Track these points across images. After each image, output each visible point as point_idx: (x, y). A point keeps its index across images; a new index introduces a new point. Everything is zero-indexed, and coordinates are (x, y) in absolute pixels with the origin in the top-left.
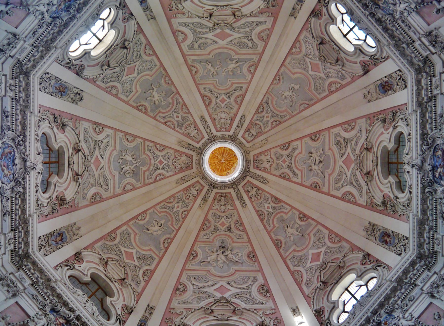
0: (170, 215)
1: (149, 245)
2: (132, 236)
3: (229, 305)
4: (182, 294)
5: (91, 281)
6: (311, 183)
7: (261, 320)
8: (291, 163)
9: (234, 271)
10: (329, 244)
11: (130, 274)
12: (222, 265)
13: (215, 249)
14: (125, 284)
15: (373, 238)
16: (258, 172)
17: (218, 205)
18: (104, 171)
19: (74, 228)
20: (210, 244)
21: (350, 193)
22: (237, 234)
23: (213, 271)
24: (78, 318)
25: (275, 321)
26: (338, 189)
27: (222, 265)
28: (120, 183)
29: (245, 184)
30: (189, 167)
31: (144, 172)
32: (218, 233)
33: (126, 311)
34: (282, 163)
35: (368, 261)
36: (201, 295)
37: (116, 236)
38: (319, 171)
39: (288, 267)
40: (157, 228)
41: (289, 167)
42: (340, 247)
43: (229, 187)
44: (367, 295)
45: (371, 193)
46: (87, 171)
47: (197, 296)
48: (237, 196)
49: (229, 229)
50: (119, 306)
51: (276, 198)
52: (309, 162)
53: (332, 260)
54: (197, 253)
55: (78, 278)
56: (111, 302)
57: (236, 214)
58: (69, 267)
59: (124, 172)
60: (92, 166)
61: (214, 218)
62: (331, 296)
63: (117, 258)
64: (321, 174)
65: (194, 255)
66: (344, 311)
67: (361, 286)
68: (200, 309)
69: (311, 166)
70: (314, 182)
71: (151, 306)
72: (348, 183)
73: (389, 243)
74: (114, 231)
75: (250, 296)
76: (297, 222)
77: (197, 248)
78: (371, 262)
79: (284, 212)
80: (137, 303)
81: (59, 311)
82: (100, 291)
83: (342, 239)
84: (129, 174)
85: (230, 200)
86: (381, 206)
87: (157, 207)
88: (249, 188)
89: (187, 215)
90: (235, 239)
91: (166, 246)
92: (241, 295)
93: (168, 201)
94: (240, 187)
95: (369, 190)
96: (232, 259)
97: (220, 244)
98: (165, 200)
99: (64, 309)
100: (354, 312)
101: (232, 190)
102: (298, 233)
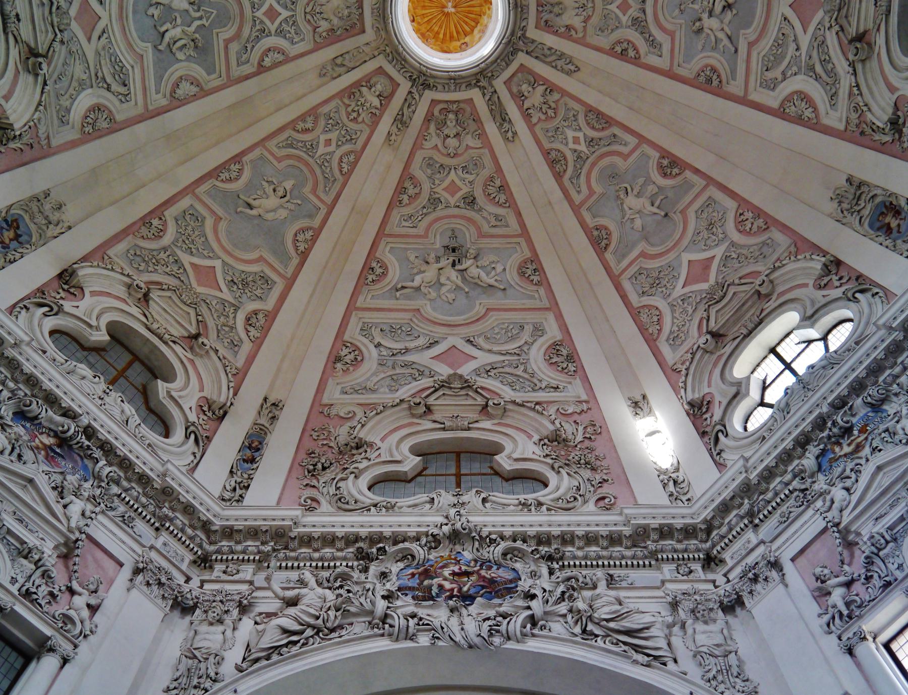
0: (307, 164)
1: (257, 247)
2: (209, 223)
3: (470, 393)
4: (351, 369)
5: (109, 343)
6: (697, 68)
7: (551, 427)
8: (644, 12)
9: (484, 311)
10: (736, 236)
11: (211, 324)
12: (451, 296)
13: (433, 255)
14: (200, 347)
15: (854, 220)
16: (550, 40)
17: (438, 135)
18: (111, 42)
19: (47, 207)
20: (419, 241)
21: (804, 97)
22: (490, 214)
23: (428, 310)
24: (89, 432)
25: (589, 430)
26: (772, 85)
27: (451, 296)
28: (161, 77)
29: (513, 75)
30: (354, 28)
31: (227, 42)
32: (439, 213)
33: (210, 414)
34: (617, 11)
35: (835, 278)
36: (398, 370)
37: (165, 224)
38: (721, 35)
39: (624, 297)
40: (272, 201)
41: (638, 23)
42: (764, 243)
43: (469, 86)
44: (824, 363)
45: (861, 94)
46: (62, 42)
48: (491, 111)
49: (470, 201)
50: (190, 401)
51: (599, 114)
52: (696, 7)
53: (740, 278)
54: (384, 267)
55: (74, 334)
56: (168, 392)
57: (487, 160)
58: (46, 309)
59: (169, 45)
60: (74, 26)
61: (429, 171)
62: (732, 368)
63: (173, 282)
64: (726, 41)
65: (379, 271)
66: (762, 404)
67: (809, 342)
68: (398, 405)
69: (700, 20)
70: (706, 66)
71: (272, 399)
72: (800, 69)
73: (895, 231)
74: (158, 211)
75: (525, 371)
76: (654, 179)
77: (385, 253)
78: (844, 281)
79: (619, 154)
80: (235, 394)
81: (36, 418)
82: (137, 366)
83: (770, 222)
84: (185, 50)
85: (471, 122)
86: (887, 130)
87: (272, 144)
88: (525, 87)
89: (354, 165)
90: (486, 228)
91: (302, 248)
92: (501, 370)
93: (299, 127)
94: (499, 84)
95: (858, 86)
96: (477, 281)
97: (446, 242)
98: (292, 125)
99: (50, 413)
100: (787, 405)
101: (475, 94)
102: (657, 211)
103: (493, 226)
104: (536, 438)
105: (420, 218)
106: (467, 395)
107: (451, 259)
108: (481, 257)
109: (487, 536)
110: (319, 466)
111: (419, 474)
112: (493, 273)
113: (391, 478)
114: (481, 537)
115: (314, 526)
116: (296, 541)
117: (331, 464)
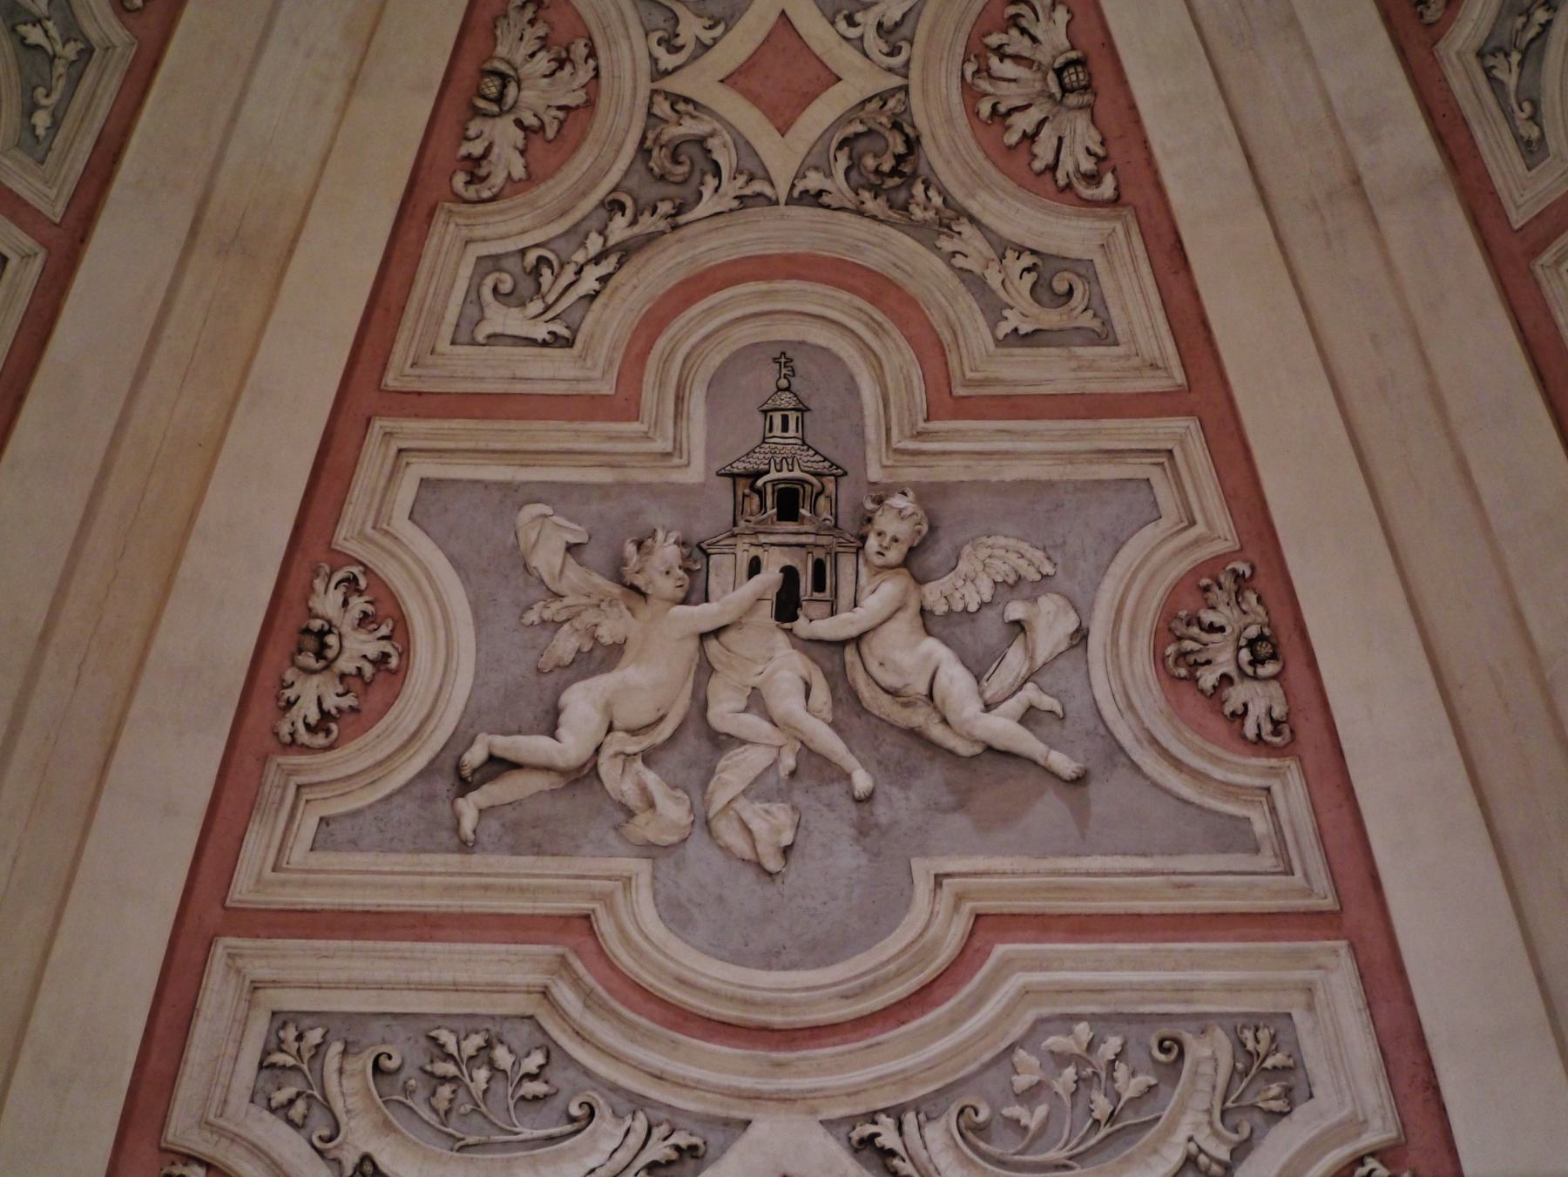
9: (958, 929)
13: (667, 552)
20: (591, 435)
22: (1002, 247)
65: (358, 647)
96: (918, 717)
103: (1018, 338)
105: (588, 283)
107: (771, 576)
108: (944, 547)
112: (1015, 661)
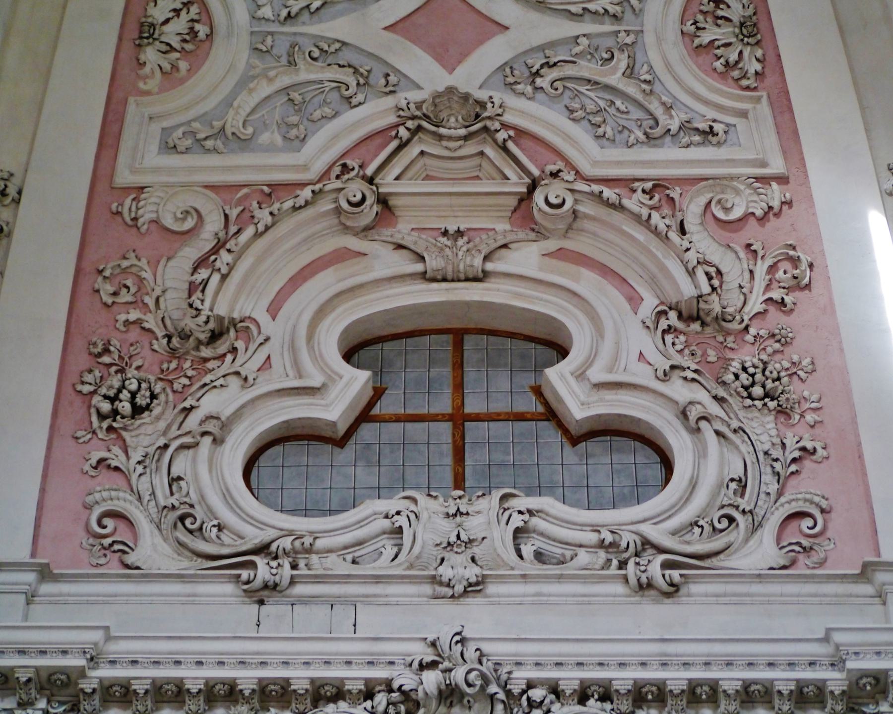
3: (490, 151)
4: (183, 65)
25: (780, 274)
47: (286, 80)
75: (630, 72)
92: (569, 71)
104: (650, 304)
106: (482, 153)
109: (524, 692)
110: (125, 407)
111: (365, 416)
113: (299, 431)
114: (508, 693)
115: (134, 662)
116: (97, 697)
117: (153, 396)
